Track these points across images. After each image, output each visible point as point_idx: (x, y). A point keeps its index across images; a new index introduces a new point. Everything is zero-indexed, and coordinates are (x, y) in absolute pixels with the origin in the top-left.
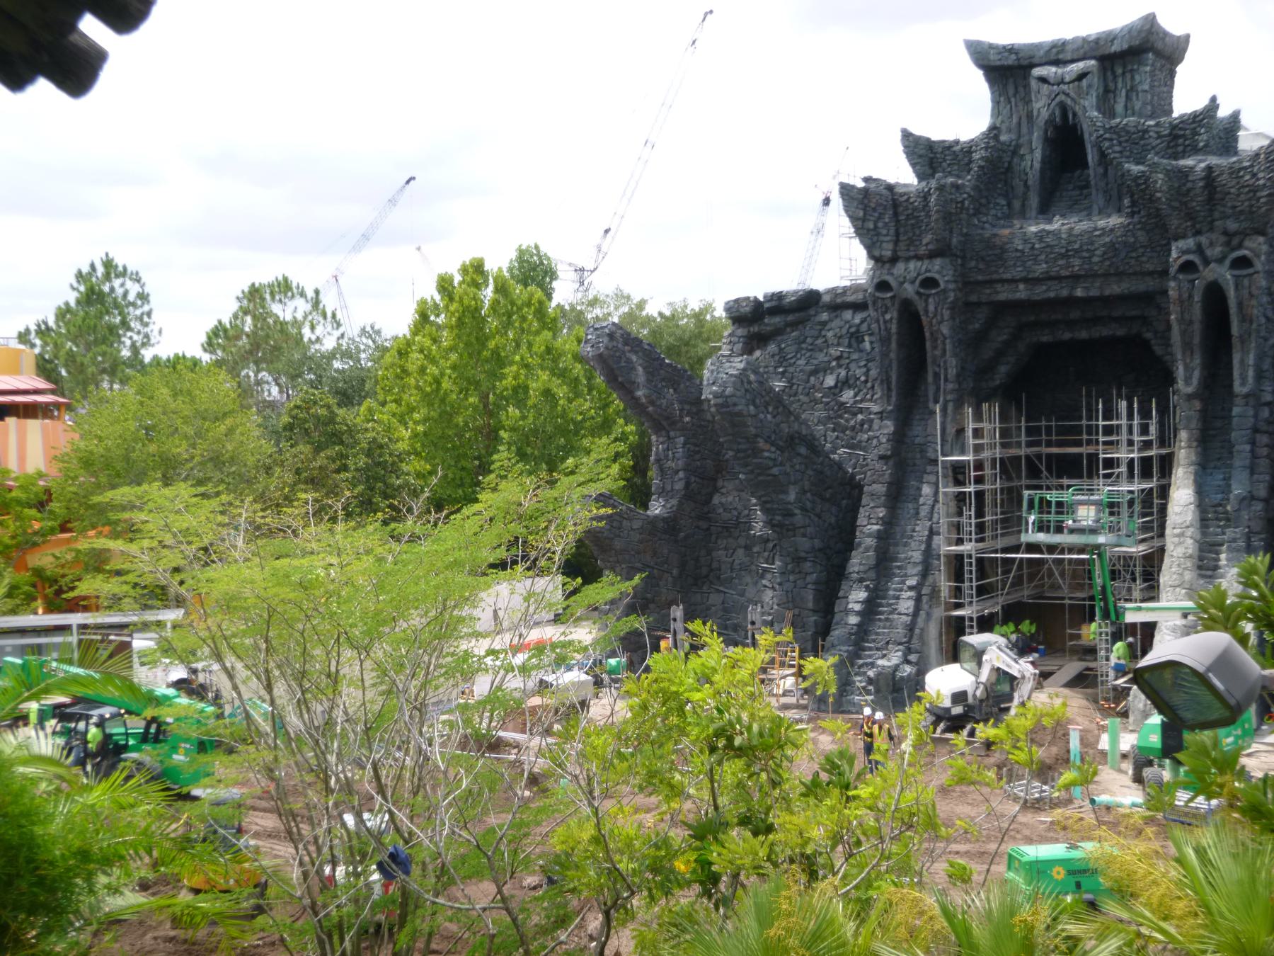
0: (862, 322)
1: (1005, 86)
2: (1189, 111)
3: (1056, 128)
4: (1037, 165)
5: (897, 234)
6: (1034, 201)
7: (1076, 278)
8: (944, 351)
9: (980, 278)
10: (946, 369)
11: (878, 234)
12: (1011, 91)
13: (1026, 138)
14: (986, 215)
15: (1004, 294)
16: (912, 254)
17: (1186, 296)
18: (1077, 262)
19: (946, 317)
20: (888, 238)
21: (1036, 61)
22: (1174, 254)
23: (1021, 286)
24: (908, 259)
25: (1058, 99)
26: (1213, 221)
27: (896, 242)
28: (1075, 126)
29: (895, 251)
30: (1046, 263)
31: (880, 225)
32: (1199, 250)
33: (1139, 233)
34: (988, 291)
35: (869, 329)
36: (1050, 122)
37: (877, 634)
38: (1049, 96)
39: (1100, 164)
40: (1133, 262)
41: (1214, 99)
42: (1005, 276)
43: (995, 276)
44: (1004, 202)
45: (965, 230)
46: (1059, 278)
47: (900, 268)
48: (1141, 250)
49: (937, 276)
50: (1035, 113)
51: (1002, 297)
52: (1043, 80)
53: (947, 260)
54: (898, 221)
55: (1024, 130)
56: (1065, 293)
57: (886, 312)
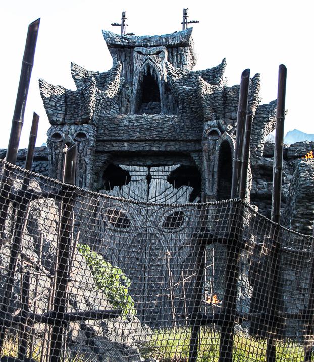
0: (37, 166)
1: (120, 57)
2: (210, 67)
3: (144, 76)
4: (135, 92)
5: (66, 111)
6: (133, 107)
7: (154, 141)
8: (86, 170)
9: (105, 138)
10: (86, 180)
11: (56, 109)
12: (123, 59)
13: (129, 80)
14: (109, 111)
15: (116, 147)
16: (73, 121)
17: (211, 147)
18: (155, 133)
19: (88, 153)
20: (61, 112)
21: (136, 44)
22: (206, 127)
23: (125, 144)
24: (70, 124)
25: (146, 62)
26: (225, 113)
27: (65, 115)
28: (153, 75)
29: (64, 119)
30: (140, 133)
31: (58, 105)
32: (219, 126)
33: (186, 121)
34: (108, 146)
35: (40, 170)
36: (142, 73)
37: (170, 75)
38: (142, 60)
39: (165, 94)
40: (183, 134)
41: (224, 60)
42: (118, 138)
43: (113, 138)
44: (118, 107)
45: (99, 114)
46: (146, 141)
47: (66, 128)
48: (187, 129)
49: (85, 132)
50: (135, 68)
51: (115, 149)
52: (140, 53)
53: (91, 126)
54: (66, 105)
55: (128, 77)
56: (147, 148)
57: (56, 149)
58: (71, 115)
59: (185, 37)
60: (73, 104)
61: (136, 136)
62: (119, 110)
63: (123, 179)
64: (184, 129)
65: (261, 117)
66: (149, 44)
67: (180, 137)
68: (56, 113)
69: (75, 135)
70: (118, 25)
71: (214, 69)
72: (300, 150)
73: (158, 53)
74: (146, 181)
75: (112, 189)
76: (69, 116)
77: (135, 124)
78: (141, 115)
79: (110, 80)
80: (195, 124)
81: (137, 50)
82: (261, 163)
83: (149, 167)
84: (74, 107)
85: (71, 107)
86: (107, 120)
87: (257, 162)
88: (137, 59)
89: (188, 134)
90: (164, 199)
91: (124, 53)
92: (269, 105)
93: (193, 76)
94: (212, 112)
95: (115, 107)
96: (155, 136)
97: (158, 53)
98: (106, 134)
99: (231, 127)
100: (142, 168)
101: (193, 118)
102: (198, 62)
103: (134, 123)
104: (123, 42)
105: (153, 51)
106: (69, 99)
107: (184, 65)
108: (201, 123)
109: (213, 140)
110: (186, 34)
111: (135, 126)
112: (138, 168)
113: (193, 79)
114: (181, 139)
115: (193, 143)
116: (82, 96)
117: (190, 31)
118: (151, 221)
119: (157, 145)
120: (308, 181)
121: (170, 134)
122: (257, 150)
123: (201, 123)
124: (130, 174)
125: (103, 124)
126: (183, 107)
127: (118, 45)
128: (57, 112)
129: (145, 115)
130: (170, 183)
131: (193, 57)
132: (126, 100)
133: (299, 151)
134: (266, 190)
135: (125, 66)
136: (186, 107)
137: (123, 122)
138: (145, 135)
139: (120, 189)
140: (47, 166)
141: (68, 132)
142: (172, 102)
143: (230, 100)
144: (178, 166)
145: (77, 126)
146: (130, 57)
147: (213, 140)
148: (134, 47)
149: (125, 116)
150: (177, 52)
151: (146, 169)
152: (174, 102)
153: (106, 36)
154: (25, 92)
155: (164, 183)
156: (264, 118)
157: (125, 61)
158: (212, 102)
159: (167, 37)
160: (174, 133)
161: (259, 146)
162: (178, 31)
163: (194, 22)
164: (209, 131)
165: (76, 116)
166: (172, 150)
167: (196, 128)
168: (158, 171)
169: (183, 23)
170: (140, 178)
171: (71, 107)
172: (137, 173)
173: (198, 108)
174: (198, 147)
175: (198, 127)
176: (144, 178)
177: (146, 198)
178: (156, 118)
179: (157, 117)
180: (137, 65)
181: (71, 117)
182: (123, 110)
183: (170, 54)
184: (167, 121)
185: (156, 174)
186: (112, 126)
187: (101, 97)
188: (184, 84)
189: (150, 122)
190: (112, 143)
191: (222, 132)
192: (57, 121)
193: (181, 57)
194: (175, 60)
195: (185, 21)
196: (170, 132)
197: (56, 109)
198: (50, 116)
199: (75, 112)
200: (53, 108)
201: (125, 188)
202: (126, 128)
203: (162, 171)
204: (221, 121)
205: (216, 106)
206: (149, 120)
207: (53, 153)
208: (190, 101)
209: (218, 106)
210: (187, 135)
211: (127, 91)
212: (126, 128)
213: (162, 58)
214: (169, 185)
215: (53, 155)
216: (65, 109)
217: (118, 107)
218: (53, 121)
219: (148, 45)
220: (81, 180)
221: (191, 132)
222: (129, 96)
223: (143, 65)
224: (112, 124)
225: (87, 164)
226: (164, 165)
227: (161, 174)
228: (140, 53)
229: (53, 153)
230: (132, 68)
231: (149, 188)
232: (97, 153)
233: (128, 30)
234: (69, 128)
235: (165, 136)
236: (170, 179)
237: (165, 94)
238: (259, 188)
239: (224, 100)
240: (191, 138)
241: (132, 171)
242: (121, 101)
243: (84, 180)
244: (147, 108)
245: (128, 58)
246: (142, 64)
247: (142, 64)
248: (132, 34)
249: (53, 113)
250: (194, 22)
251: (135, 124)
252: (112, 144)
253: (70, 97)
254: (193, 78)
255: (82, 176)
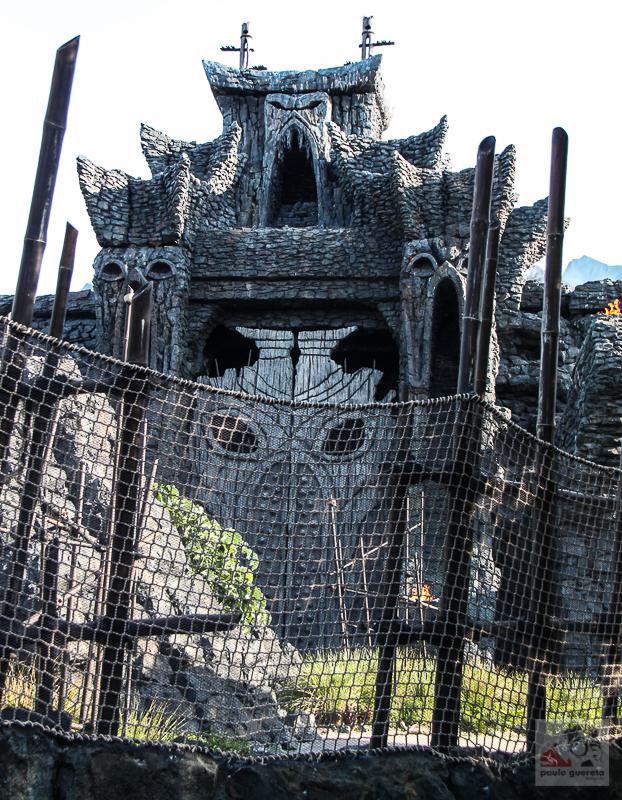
0: (73, 330)
1: (238, 112)
2: (417, 133)
3: (286, 151)
4: (267, 182)
5: (130, 220)
6: (263, 213)
7: (304, 279)
8: (170, 338)
9: (208, 274)
10: (170, 357)
11: (112, 217)
12: (244, 117)
13: (256, 159)
14: (217, 220)
15: (230, 292)
16: (144, 241)
17: (419, 292)
18: (306, 264)
19: (175, 304)
20: (121, 223)
21: (269, 88)
22: (409, 252)
23: (249, 286)
24: (139, 246)
25: (290, 123)
26: (447, 224)
27: (129, 228)
28: (304, 149)
29: (126, 236)
30: (277, 263)
31: (114, 208)
32: (433, 250)
33: (368, 240)
34: (214, 289)
35: (80, 336)
36: (282, 144)
37: (336, 148)
38: (282, 120)
39: (326, 186)
40: (362, 266)
41: (443, 120)
42: (233, 274)
43: (224, 273)
44: (233, 213)
45: (197, 227)
46: (288, 279)
47: (130, 253)
48: (370, 256)
49: (169, 263)
50: (267, 135)
51: (229, 295)
52: (277, 105)
53: (180, 250)
54: (132, 208)
55: (254, 153)
56: (292, 294)
57: (112, 296)
58: (141, 229)
59: (367, 74)
60: (145, 207)
61: (269, 270)
62: (237, 219)
63: (244, 354)
64: (364, 256)
65: (518, 232)
66: (294, 87)
67: (356, 271)
68: (110, 224)
69: (148, 267)
70: (234, 49)
71: (425, 136)
72: (594, 298)
73: (313, 105)
74: (289, 359)
75: (222, 374)
76: (137, 230)
77: (268, 246)
78: (280, 228)
79: (218, 159)
80: (386, 245)
81: (271, 100)
82: (516, 323)
83: (296, 331)
84: (146, 212)
85: (141, 213)
86: (212, 238)
87: (509, 321)
88: (272, 116)
89: (373, 265)
90: (324, 396)
91: (245, 106)
92: (533, 208)
93: (383, 151)
94: (421, 223)
95: (227, 213)
96: (307, 269)
97: (313, 105)
98: (210, 266)
99: (458, 253)
100: (280, 334)
101: (383, 233)
102: (392, 123)
103: (265, 244)
104: (243, 83)
105: (303, 100)
106: (136, 197)
107: (365, 130)
108: (398, 243)
109: (422, 278)
110: (368, 68)
111: (268, 249)
112: (273, 334)
113: (383, 157)
114: (358, 276)
115: (381, 283)
116: (163, 191)
117: (376, 61)
118: (298, 439)
119: (311, 288)
120: (610, 360)
121: (337, 266)
122: (510, 299)
123: (398, 243)
124: (258, 344)
125: (204, 246)
126: (362, 212)
127: (233, 88)
128: (114, 222)
129: (287, 229)
130: (337, 363)
131: (382, 114)
132: (250, 198)
133: (592, 299)
134: (526, 377)
135: (247, 130)
136: (368, 212)
137: (244, 242)
138: (288, 269)
139: (238, 376)
140: (93, 330)
141: (136, 261)
142: (341, 202)
143: (455, 198)
144: (353, 328)
145: (153, 250)
146: (257, 113)
147: (422, 278)
148: (265, 93)
149: (248, 230)
150: (351, 103)
151: (290, 334)
152: (344, 202)
153: (211, 71)
154: (50, 183)
155: (325, 363)
156: (522, 234)
157: (247, 122)
158: (420, 201)
159: (330, 74)
160: (344, 264)
161: (513, 289)
162: (353, 61)
163: (384, 43)
164: (414, 260)
165: (151, 230)
166: (341, 297)
167: (389, 253)
168: (313, 340)
169: (363, 46)
170: (278, 353)
171: (141, 213)
172: (272, 344)
173: (392, 215)
174: (392, 292)
175: (393, 253)
176: (285, 353)
177: (289, 392)
178: (309, 235)
179: (311, 232)
180: (270, 128)
181: (140, 232)
182: (244, 217)
183: (337, 108)
184: (330, 240)
185: (308, 344)
186: (221, 250)
187: (201, 193)
188: (365, 166)
189: (297, 242)
190: (222, 283)
191: (440, 262)
192: (113, 239)
193: (358, 114)
194: (347, 120)
195: (367, 42)
196: (337, 262)
197: (112, 217)
198: (100, 231)
199: (148, 222)
200: (106, 214)
201: (248, 373)
202: (249, 253)
203: (321, 340)
204: (438, 240)
205: (428, 210)
206: (295, 238)
207: (106, 303)
208: (376, 199)
209: (432, 211)
210: (371, 267)
211: (252, 181)
212: (249, 253)
213: (320, 115)
214: (335, 366)
215: (106, 307)
216: (130, 217)
217: (233, 213)
218: (105, 239)
219: (292, 89)
220: (161, 357)
221: (377, 261)
222: (255, 191)
223: (284, 129)
224: (222, 246)
225: (172, 326)
226: (325, 328)
227: (318, 346)
228: (277, 105)
229: (106, 303)
230: (261, 134)
231: (295, 373)
232: (192, 303)
233: (253, 60)
234: (137, 254)
235: (326, 270)
236: (336, 355)
237: (326, 186)
238: (513, 373)
239: (443, 199)
240: (378, 274)
241: (261, 340)
242: (240, 201)
243: (166, 358)
244: (291, 214)
245: (253, 116)
246: (281, 128)
247: (281, 128)
248: (262, 68)
249: (106, 225)
250: (384, 43)
251: (268, 246)
252: (222, 286)
253: (140, 192)
254: (382, 154)
255: (161, 349)
